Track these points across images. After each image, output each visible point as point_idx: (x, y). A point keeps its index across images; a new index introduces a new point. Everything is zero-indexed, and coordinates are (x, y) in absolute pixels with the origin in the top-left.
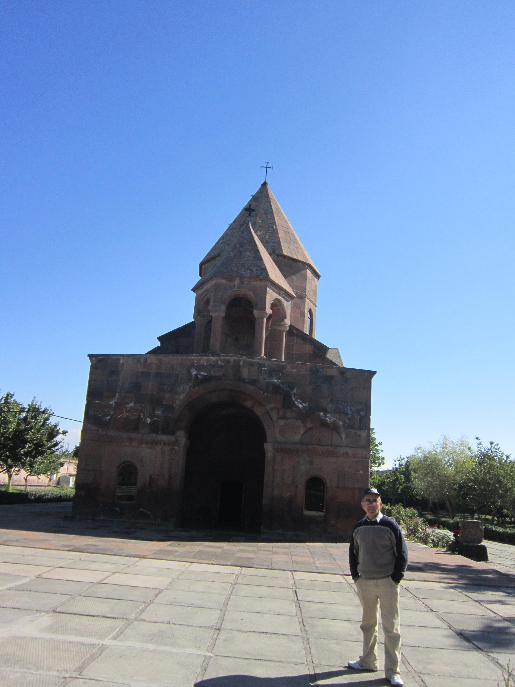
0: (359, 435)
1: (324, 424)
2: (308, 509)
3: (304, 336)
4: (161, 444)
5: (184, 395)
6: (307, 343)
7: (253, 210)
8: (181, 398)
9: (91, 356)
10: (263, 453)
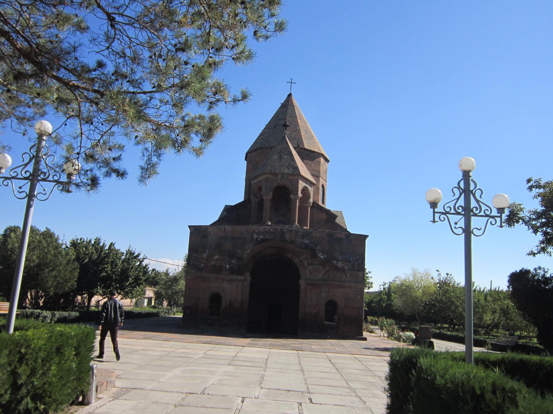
0: (358, 275)
1: (337, 268)
2: (326, 320)
4: (236, 281)
5: (250, 250)
7: (288, 126)
8: (248, 252)
9: (190, 227)
10: (298, 286)
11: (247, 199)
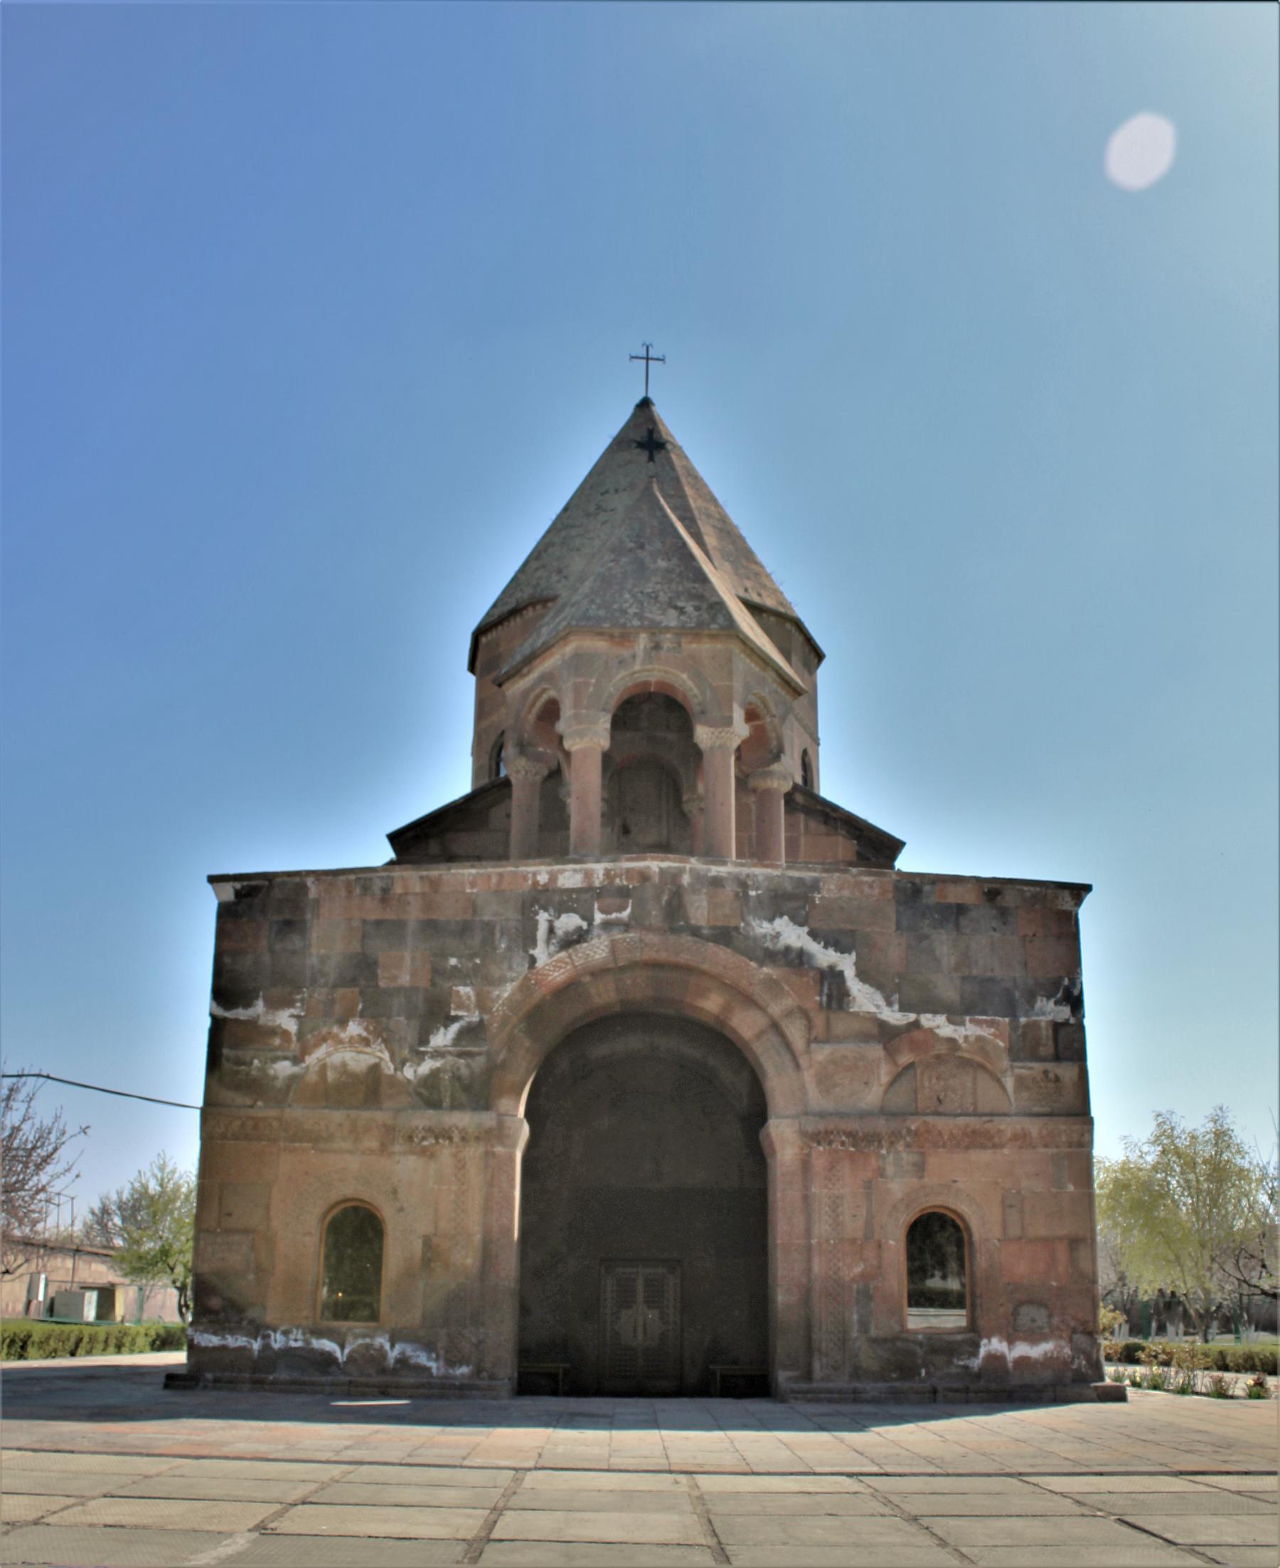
0: (1057, 1079)
3: (828, 810)
4: (450, 1139)
11: (485, 781)
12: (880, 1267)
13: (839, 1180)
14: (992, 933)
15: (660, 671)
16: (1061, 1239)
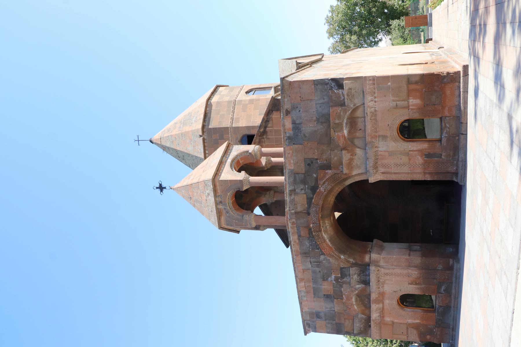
3: (264, 121)
6: (270, 118)
9: (306, 333)
12: (419, 151)
13: (389, 164)
14: (301, 111)
15: (228, 201)
16: (408, 87)
